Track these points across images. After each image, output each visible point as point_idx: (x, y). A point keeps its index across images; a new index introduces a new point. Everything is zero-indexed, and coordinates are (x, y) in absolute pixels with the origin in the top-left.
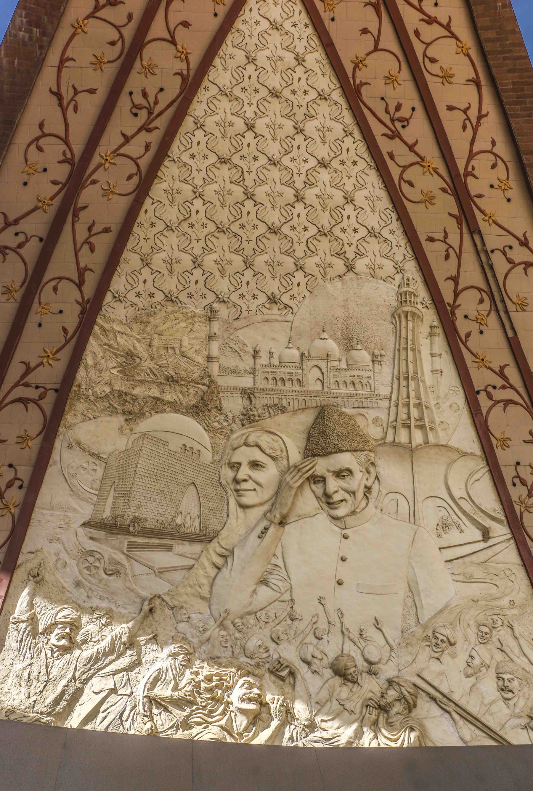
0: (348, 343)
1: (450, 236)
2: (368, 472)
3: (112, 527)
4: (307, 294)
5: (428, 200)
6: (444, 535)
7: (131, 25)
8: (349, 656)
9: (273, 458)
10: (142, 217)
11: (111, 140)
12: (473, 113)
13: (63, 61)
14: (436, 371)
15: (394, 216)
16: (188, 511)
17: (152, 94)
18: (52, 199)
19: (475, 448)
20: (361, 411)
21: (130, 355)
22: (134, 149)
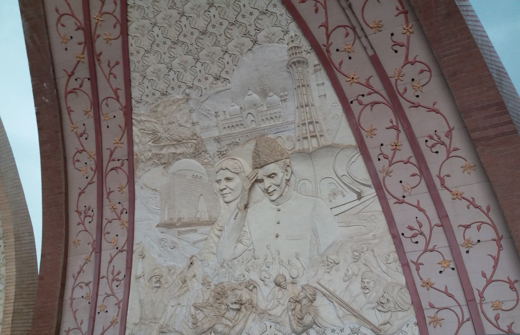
0: (264, 93)
3: (168, 226)
6: (333, 201)
9: (237, 174)
14: (321, 96)
21: (154, 132)
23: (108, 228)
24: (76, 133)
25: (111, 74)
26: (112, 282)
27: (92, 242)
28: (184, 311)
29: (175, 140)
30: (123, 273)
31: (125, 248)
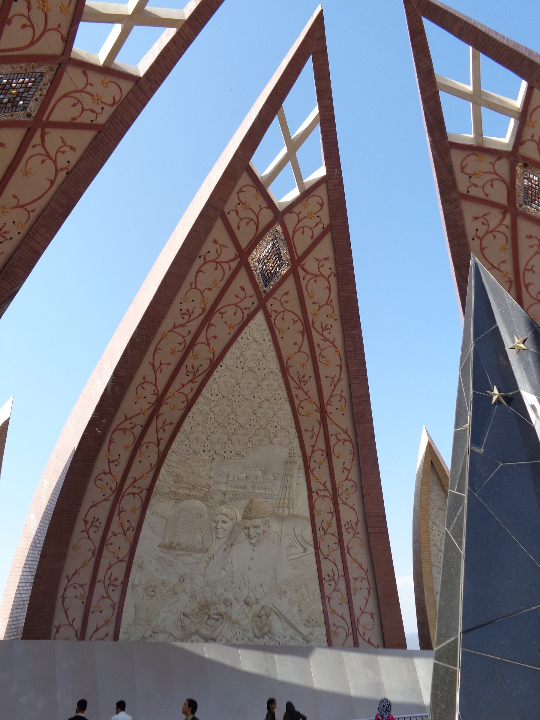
0: (265, 472)
2: (266, 525)
4: (252, 451)
7: (189, 336)
10: (187, 419)
12: (336, 380)
13: (156, 350)
15: (293, 421)
19: (308, 515)
21: (178, 476)
23: (113, 540)
24: (109, 460)
26: (108, 587)
27: (93, 549)
30: (121, 579)
31: (126, 559)
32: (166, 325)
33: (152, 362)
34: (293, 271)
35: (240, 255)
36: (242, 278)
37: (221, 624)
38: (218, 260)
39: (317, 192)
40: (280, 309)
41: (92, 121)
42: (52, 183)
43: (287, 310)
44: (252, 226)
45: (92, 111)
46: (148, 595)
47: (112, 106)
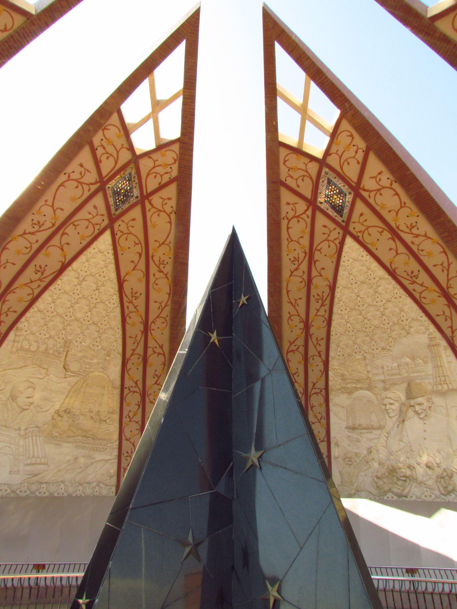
0: (413, 358)
1: (446, 312)
2: (429, 401)
3: (353, 428)
4: (395, 344)
5: (433, 301)
8: (431, 462)
10: (332, 333)
11: (313, 312)
12: (446, 264)
13: (288, 292)
15: (421, 311)
16: (374, 420)
17: (320, 294)
18: (302, 334)
20: (424, 381)
21: (342, 375)
22: (322, 312)
25: (317, 343)
28: (370, 479)
29: (356, 380)
31: (326, 439)
32: (286, 273)
33: (289, 301)
34: (357, 195)
35: (310, 205)
36: (320, 220)
37: (409, 484)
38: (297, 215)
39: (341, 128)
40: (363, 228)
41: (170, 178)
42: (170, 223)
43: (369, 227)
44: (307, 180)
45: (166, 173)
46: (347, 464)
47: (175, 163)
